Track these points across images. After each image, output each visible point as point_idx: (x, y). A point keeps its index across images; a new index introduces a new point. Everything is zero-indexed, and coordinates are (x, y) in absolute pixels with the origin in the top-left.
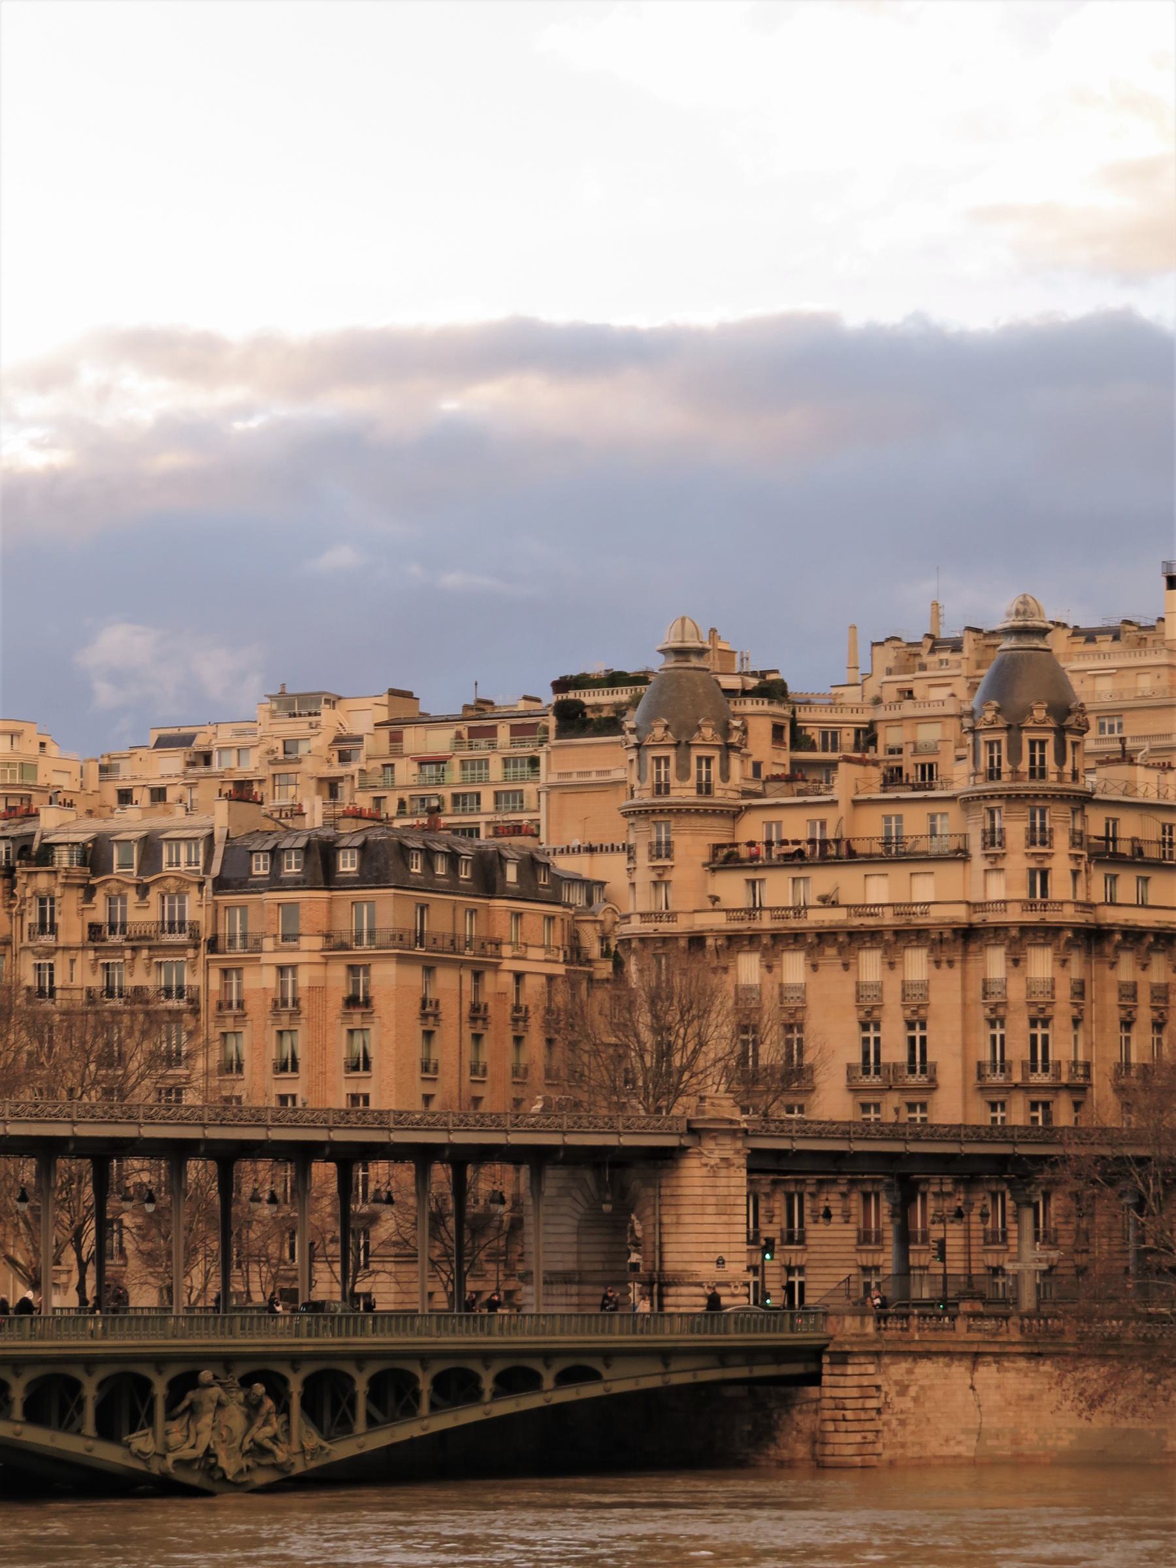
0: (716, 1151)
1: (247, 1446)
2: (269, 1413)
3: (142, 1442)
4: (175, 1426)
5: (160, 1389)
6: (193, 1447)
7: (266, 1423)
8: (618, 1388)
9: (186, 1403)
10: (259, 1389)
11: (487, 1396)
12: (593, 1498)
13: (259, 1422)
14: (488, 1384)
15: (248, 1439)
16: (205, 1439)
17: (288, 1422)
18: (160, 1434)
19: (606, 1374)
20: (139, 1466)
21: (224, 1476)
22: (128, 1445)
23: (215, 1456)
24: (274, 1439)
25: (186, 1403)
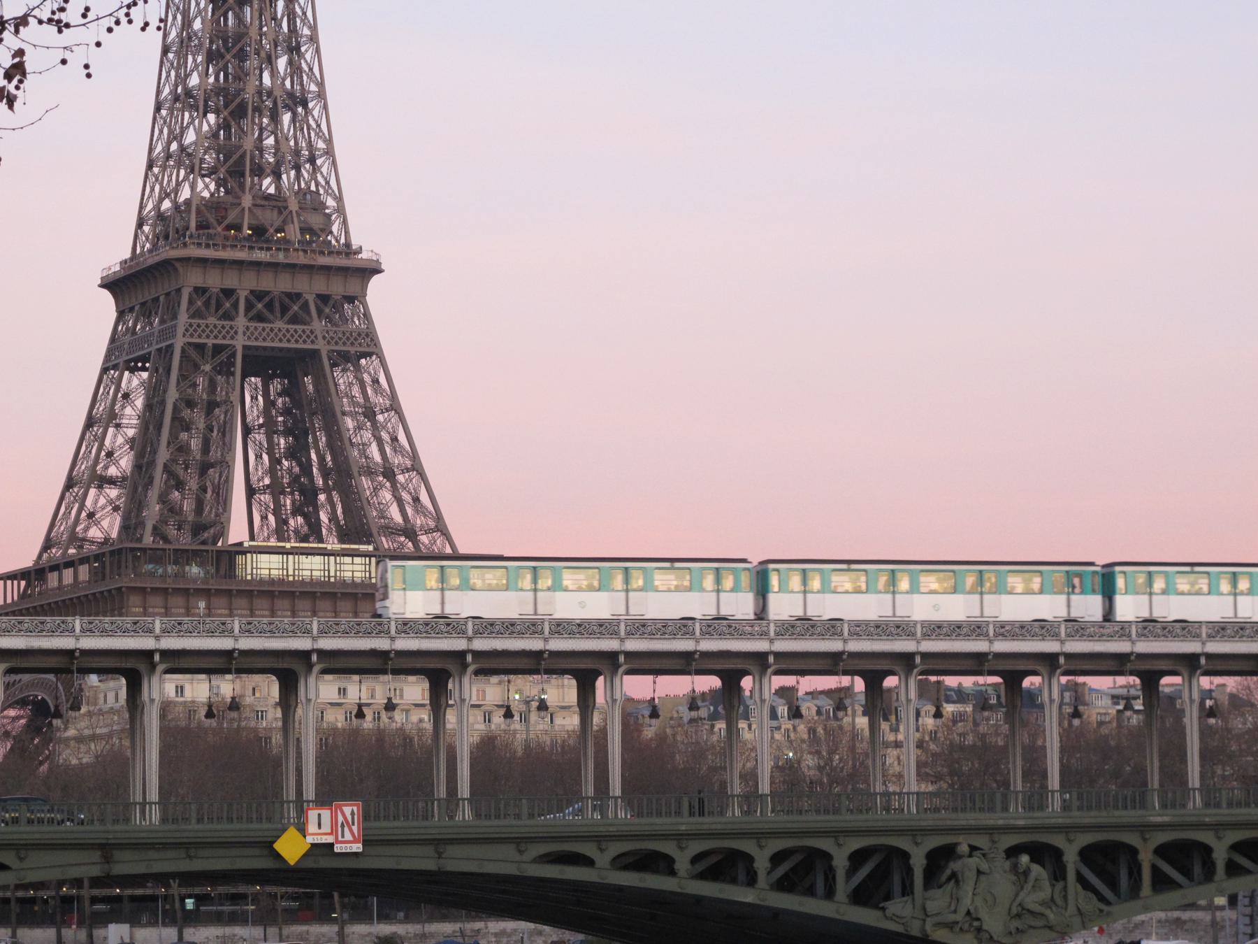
1: (1014, 911)
3: (898, 906)
5: (918, 862)
6: (955, 912)
9: (948, 872)
10: (1025, 859)
13: (1029, 886)
15: (1015, 905)
17: (1065, 888)
18: (918, 901)
21: (991, 937)
22: (883, 909)
25: (948, 872)
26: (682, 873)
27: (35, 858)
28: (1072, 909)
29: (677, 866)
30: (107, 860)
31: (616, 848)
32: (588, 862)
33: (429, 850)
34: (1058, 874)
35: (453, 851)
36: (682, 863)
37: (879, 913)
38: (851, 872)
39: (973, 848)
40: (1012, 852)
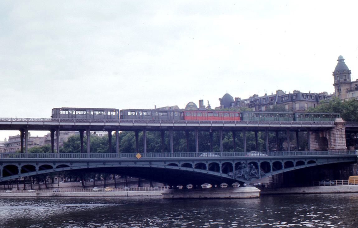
0: (340, 127)
1: (250, 174)
2: (254, 169)
4: (237, 171)
5: (234, 165)
6: (240, 174)
7: (254, 170)
8: (319, 164)
10: (252, 164)
11: (295, 166)
12: (73, 197)
14: (295, 164)
16: (242, 173)
17: (258, 170)
18: (234, 173)
19: (317, 162)
20: (231, 178)
22: (228, 174)
23: (244, 176)
24: (256, 173)
26: (193, 168)
27: (74, 165)
28: (260, 175)
29: (193, 166)
30: (88, 165)
31: (182, 163)
32: (177, 165)
33: (148, 163)
34: (257, 168)
35: (153, 163)
36: (193, 166)
37: (227, 175)
38: (222, 167)
39: (243, 163)
40: (250, 163)
